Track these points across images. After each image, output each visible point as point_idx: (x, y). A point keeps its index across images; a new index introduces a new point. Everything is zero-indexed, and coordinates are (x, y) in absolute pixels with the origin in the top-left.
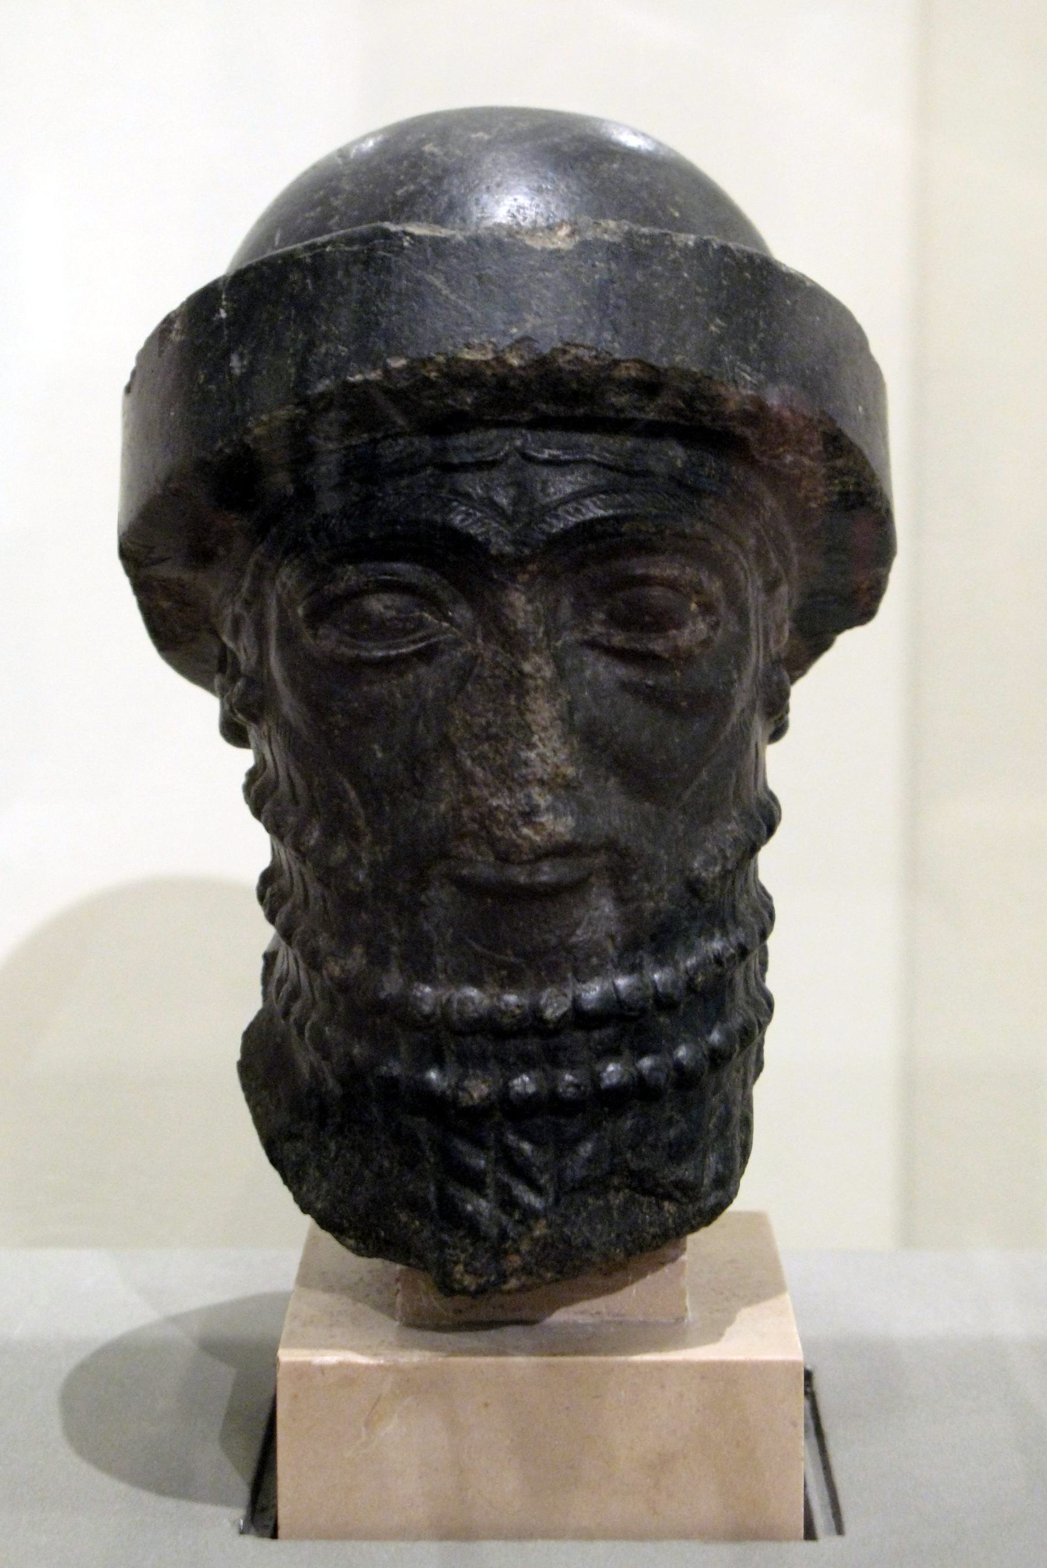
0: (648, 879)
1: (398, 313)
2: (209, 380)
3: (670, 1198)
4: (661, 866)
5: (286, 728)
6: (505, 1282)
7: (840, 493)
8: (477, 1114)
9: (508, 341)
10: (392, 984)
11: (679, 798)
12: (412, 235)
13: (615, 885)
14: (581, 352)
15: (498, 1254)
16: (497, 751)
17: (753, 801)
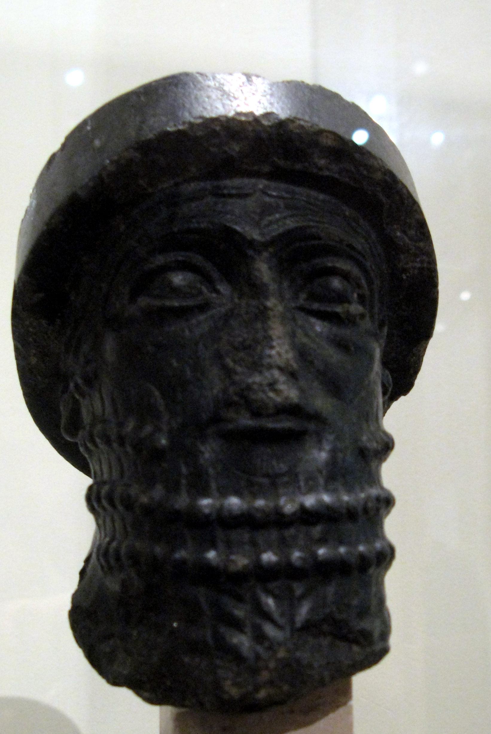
3: (357, 643)
7: (419, 269)
8: (240, 577)
10: (182, 501)
15: (255, 671)
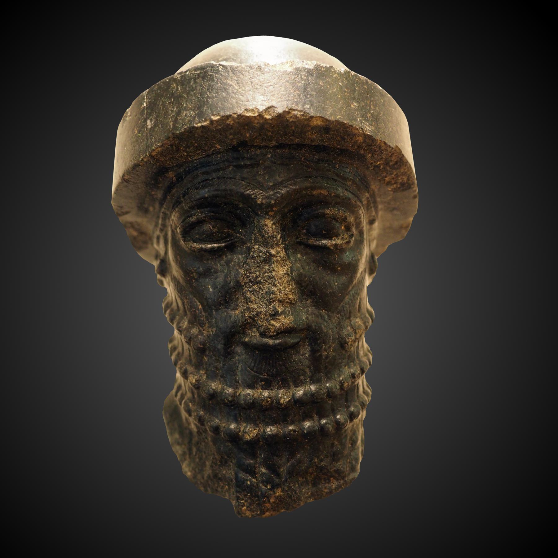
0: (324, 343)
1: (216, 97)
2: (139, 132)
4: (330, 337)
5: (174, 279)
6: (264, 514)
9: (264, 108)
11: (337, 308)
12: (223, 66)
13: (310, 345)
14: (296, 112)
16: (260, 288)
17: (366, 310)
